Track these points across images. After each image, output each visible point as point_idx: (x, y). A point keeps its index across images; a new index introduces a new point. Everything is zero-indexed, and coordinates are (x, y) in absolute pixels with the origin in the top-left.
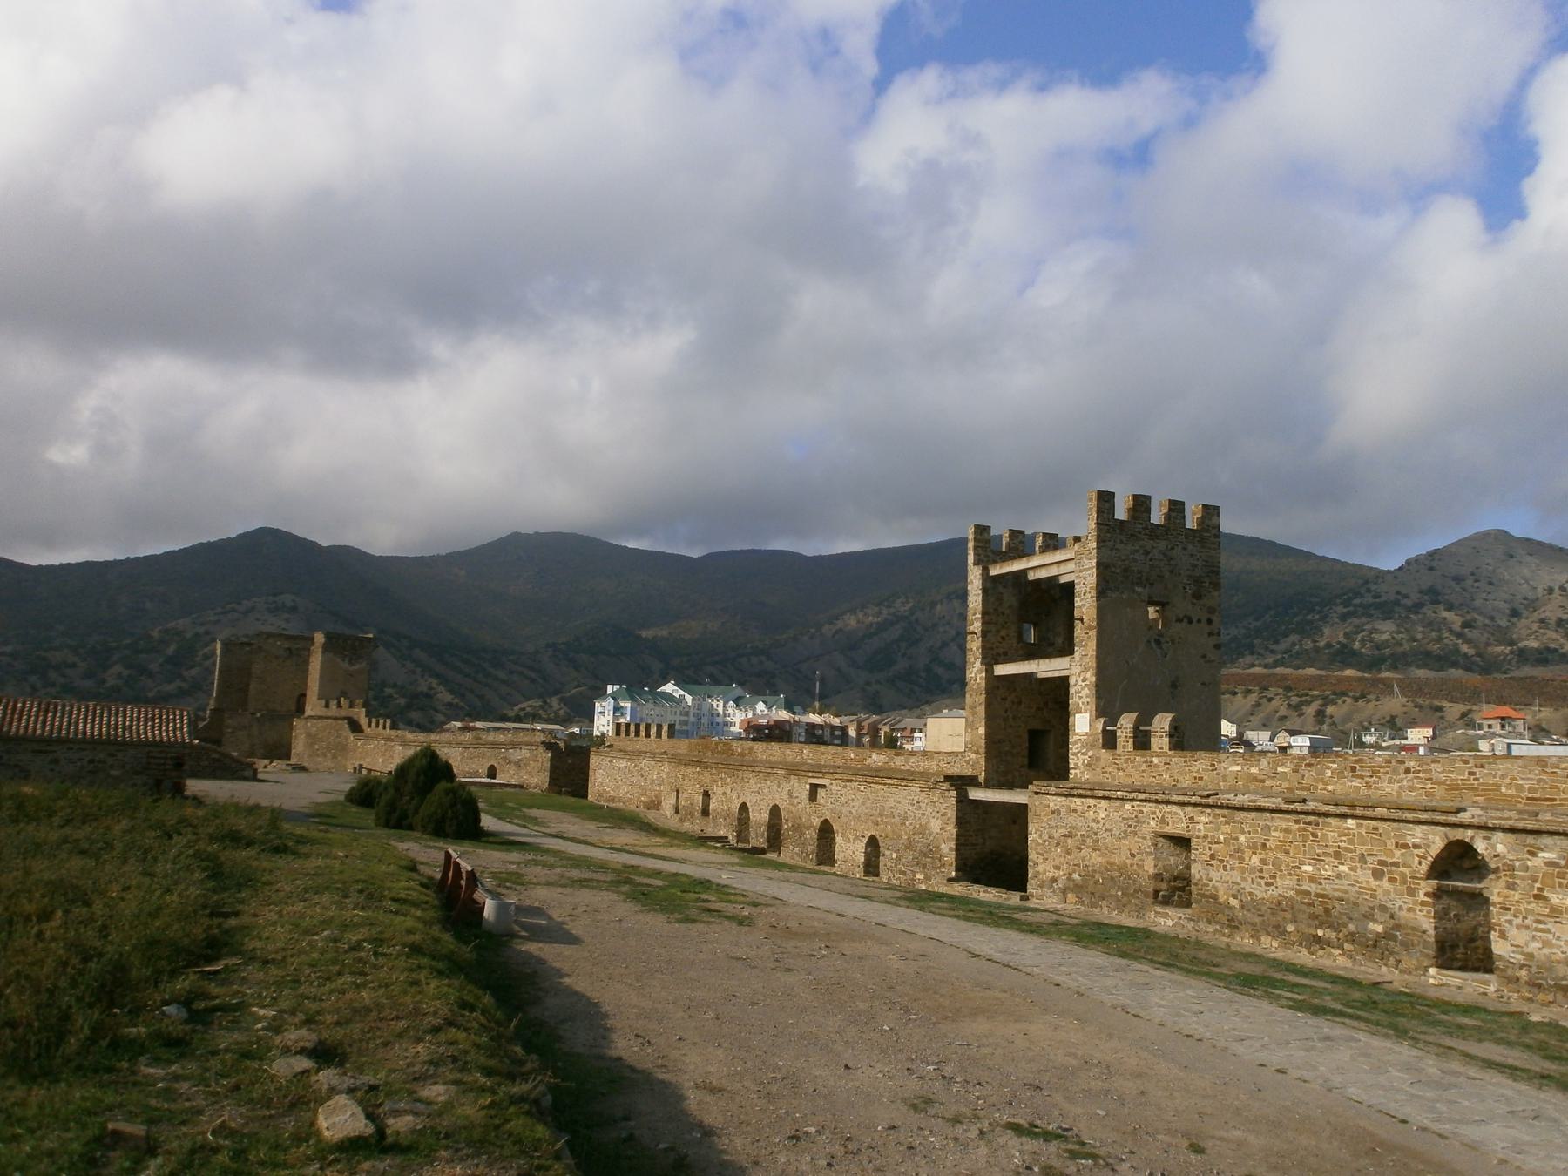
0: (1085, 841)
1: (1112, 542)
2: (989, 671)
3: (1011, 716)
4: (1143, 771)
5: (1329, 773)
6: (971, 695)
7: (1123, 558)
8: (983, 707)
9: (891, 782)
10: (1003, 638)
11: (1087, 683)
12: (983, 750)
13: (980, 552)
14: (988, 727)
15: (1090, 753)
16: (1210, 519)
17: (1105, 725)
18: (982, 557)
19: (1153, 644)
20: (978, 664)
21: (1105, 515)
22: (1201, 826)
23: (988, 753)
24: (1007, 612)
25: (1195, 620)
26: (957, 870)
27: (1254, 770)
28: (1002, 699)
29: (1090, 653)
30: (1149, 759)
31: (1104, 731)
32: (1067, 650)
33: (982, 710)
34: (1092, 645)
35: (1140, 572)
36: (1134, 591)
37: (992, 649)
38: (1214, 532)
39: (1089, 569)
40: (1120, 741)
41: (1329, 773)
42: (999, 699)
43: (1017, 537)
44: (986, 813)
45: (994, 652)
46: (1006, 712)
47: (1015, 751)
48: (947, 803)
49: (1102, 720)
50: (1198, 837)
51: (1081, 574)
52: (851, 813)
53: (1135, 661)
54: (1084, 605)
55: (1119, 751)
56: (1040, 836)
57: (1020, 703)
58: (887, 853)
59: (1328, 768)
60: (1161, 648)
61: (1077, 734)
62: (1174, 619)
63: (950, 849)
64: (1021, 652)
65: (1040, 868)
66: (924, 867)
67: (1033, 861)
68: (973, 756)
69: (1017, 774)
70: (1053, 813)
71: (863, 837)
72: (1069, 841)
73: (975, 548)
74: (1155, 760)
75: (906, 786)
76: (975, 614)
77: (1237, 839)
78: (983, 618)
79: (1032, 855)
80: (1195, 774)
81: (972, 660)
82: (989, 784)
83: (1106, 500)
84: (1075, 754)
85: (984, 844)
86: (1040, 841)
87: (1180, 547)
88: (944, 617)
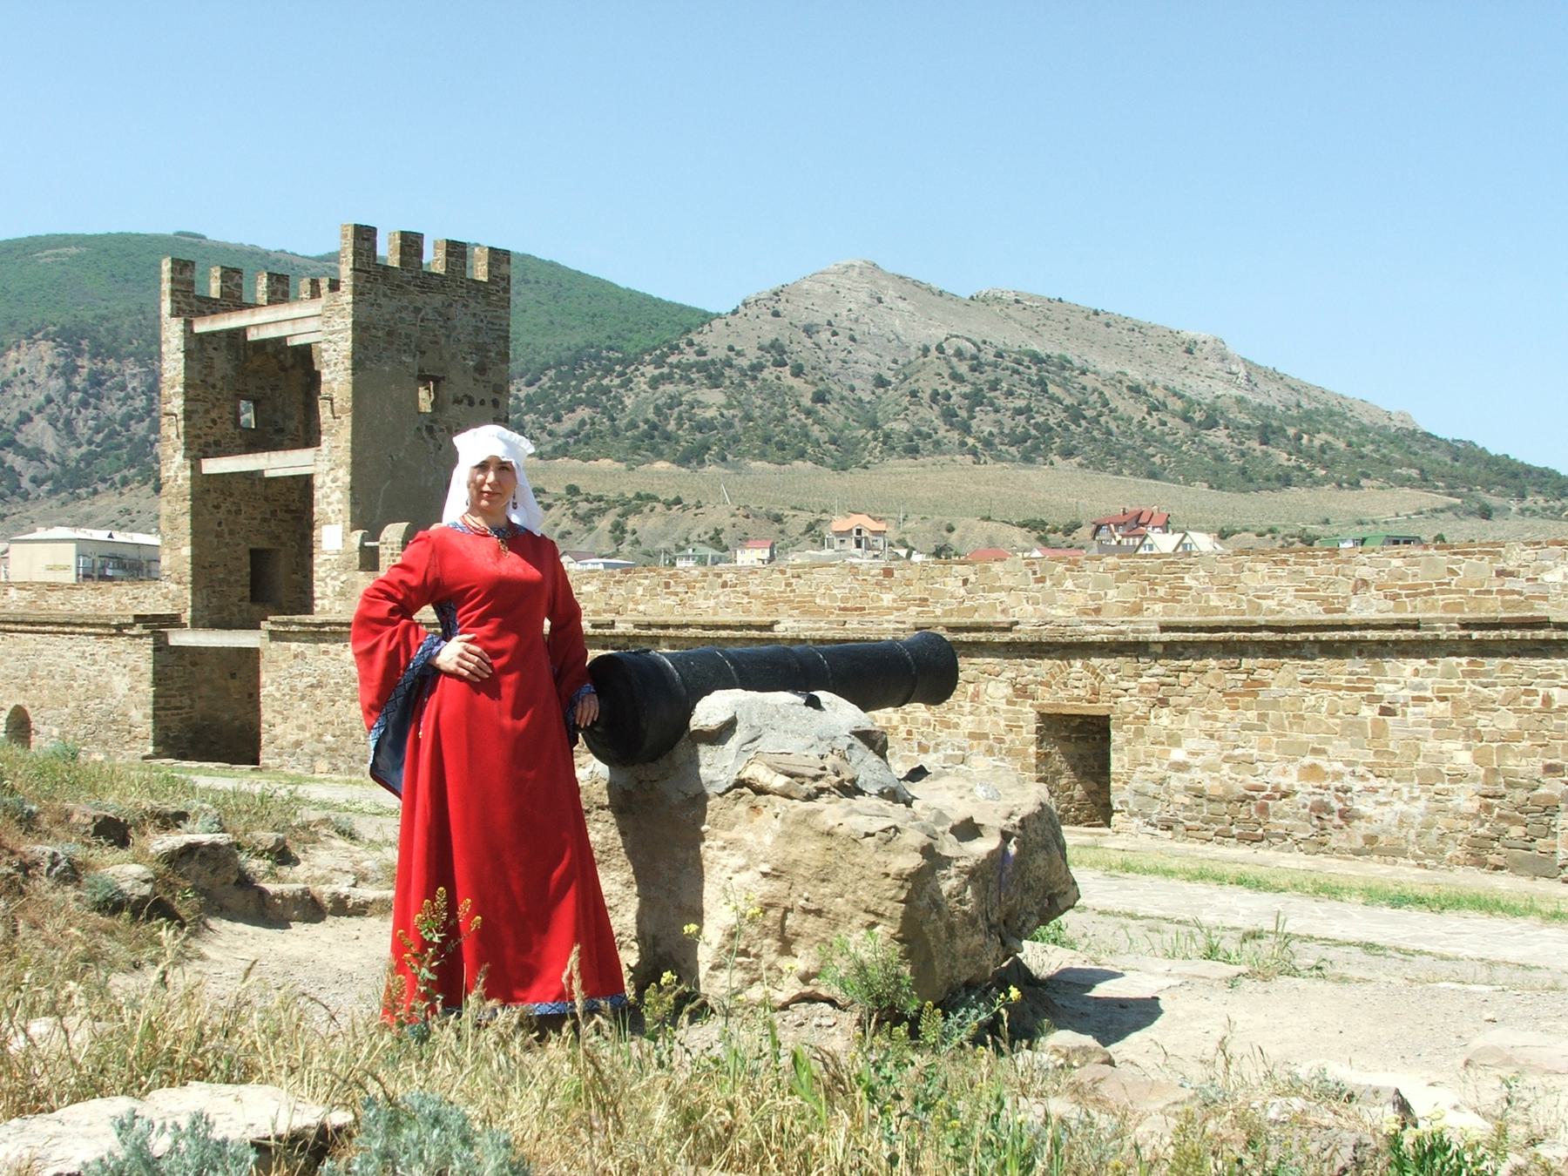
0: (340, 691)
1: (372, 295)
2: (196, 468)
3: (226, 531)
5: (640, 591)
6: (169, 502)
7: (387, 317)
8: (188, 518)
9: (49, 628)
10: (214, 422)
11: (339, 483)
13: (180, 298)
14: (194, 544)
15: (343, 578)
16: (498, 268)
17: (364, 538)
18: (183, 305)
19: (425, 434)
20: (179, 458)
21: (364, 259)
23: (194, 582)
24: (220, 384)
25: (477, 401)
26: (156, 744)
28: (214, 507)
31: (362, 548)
32: (309, 436)
33: (185, 522)
34: (346, 434)
35: (408, 336)
36: (401, 363)
37: (198, 437)
38: (503, 284)
39: (339, 331)
41: (640, 591)
42: (210, 506)
43: (232, 279)
44: (194, 664)
45: (202, 441)
46: (220, 524)
47: (232, 579)
48: (140, 655)
49: (359, 533)
51: (330, 337)
53: (401, 454)
54: (335, 379)
56: (278, 689)
57: (238, 512)
58: (44, 729)
59: (639, 585)
60: (433, 438)
62: (451, 398)
63: (145, 716)
64: (239, 441)
65: (278, 730)
66: (105, 743)
67: (267, 722)
68: (174, 587)
69: (235, 610)
70: (296, 656)
72: (318, 692)
73: (173, 292)
75: (72, 633)
76: (173, 387)
78: (186, 393)
79: (266, 715)
81: (170, 452)
82: (196, 624)
83: (364, 236)
84: (323, 580)
85: (191, 707)
86: (278, 695)
87: (460, 304)
88: (23, 371)
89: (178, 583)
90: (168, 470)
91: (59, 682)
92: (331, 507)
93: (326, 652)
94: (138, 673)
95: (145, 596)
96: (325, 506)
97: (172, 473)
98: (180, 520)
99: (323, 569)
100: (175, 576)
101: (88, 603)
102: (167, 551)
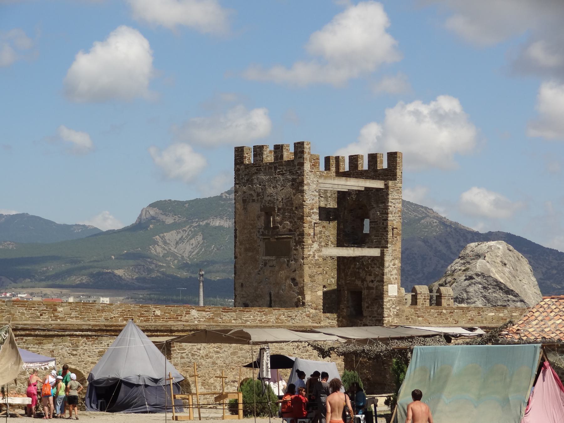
4: (436, 317)
6: (310, 268)
11: (395, 266)
15: (398, 308)
27: (501, 315)
29: (398, 250)
30: (440, 311)
34: (399, 245)
52: (214, 363)
55: (418, 307)
71: (234, 382)
74: (444, 311)
76: (312, 209)
80: (469, 318)
84: (389, 309)
89: (316, 309)
90: (309, 251)
92: (392, 276)
95: (296, 316)
97: (311, 253)
99: (389, 304)
100: (314, 305)
101: (256, 319)
102: (309, 292)
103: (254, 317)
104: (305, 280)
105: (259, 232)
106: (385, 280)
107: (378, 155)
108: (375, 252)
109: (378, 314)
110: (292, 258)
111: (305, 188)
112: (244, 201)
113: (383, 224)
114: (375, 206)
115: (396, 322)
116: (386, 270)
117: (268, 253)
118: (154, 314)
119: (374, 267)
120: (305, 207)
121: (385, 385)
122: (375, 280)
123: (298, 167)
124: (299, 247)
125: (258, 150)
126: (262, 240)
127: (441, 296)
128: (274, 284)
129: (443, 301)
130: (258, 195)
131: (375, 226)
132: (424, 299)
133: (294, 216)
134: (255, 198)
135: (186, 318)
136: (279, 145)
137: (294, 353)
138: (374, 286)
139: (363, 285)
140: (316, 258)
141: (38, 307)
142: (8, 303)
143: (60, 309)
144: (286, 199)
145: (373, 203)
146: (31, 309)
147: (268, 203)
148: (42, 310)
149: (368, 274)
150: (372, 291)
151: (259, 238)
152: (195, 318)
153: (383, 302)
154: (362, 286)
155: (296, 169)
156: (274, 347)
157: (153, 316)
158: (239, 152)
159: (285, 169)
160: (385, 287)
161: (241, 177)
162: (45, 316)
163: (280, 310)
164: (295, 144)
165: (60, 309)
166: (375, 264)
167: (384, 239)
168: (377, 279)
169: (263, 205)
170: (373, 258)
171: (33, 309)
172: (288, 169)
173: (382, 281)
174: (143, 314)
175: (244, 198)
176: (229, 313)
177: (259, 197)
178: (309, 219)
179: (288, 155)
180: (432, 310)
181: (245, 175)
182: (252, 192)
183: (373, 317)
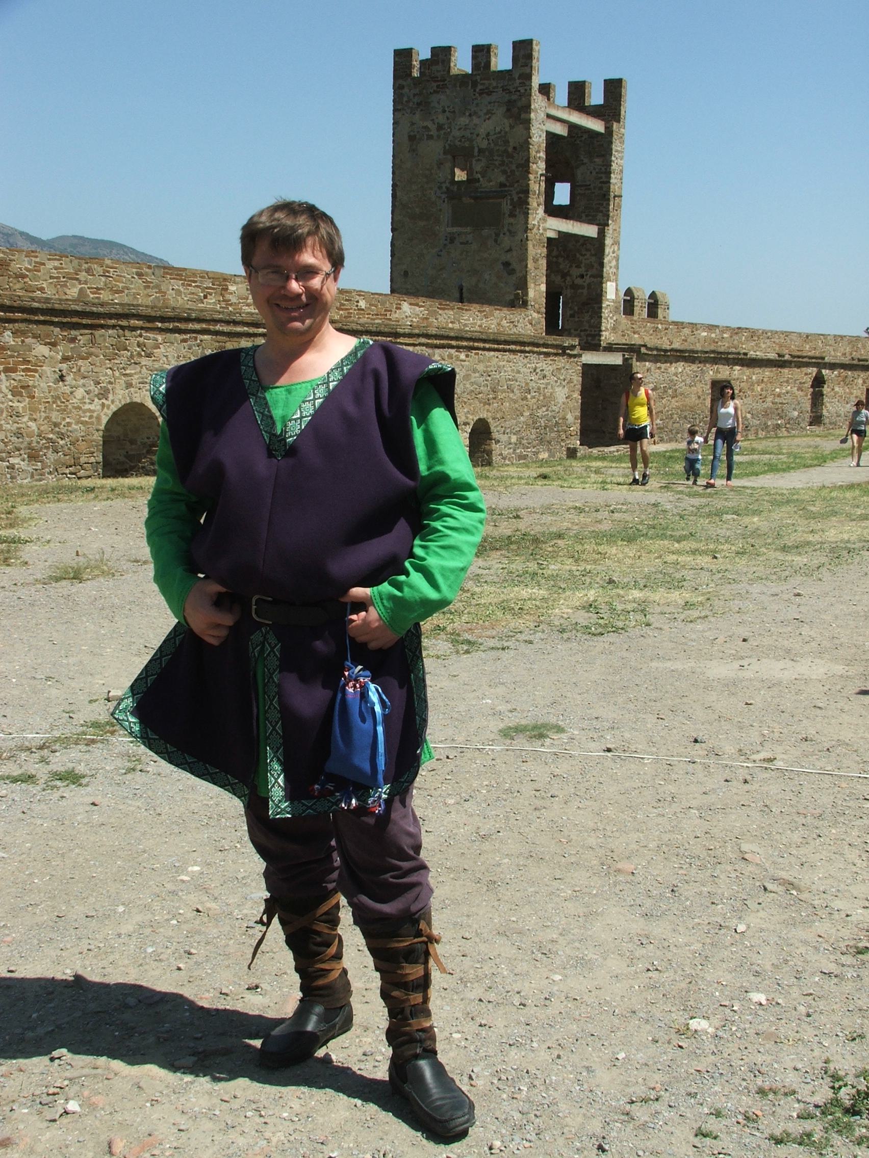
4: (651, 335)
6: (534, 246)
9: (513, 347)
12: (544, 310)
15: (615, 318)
22: (736, 372)
27: (713, 335)
30: (656, 326)
40: (637, 310)
50: (734, 380)
55: (635, 318)
61: (607, 300)
63: (575, 419)
74: (660, 326)
76: (538, 152)
77: (751, 378)
80: (683, 338)
89: (538, 313)
90: (534, 219)
91: (517, 394)
93: (660, 368)
94: (572, 385)
96: (608, 268)
97: (536, 222)
98: (540, 262)
102: (532, 285)
103: (473, 320)
104: (529, 266)
105: (440, 188)
106: (605, 275)
107: (587, 84)
108: (590, 231)
109: (590, 326)
110: (505, 229)
111: (532, 115)
112: (412, 138)
113: (601, 188)
114: (586, 161)
115: (613, 338)
116: (606, 261)
117: (455, 222)
118: (357, 306)
119: (585, 255)
120: (531, 147)
121: (604, 432)
122: (587, 275)
123: (521, 81)
124: (518, 210)
125: (442, 54)
126: (446, 202)
127: (658, 305)
128: (468, 271)
129: (660, 311)
130: (440, 127)
131: (587, 192)
132: (641, 307)
133: (511, 162)
134: (434, 132)
135: (397, 316)
136: (483, 46)
137: (531, 380)
138: (585, 284)
139: (565, 281)
140: (541, 231)
141: (201, 282)
142: (157, 272)
143: (232, 288)
144: (495, 134)
145: (582, 158)
146: (190, 285)
147: (460, 141)
148: (207, 288)
149: (574, 265)
150: (580, 291)
151: (440, 197)
152: (407, 317)
153: (601, 308)
154: (563, 284)
155: (515, 85)
156: (509, 369)
157: (355, 310)
158: (403, 57)
159: (495, 84)
160: (604, 285)
161: (405, 99)
162: (211, 299)
163: (501, 310)
164: (514, 43)
165: (232, 288)
166: (587, 250)
167: (602, 212)
168: (589, 273)
169: (450, 145)
170: (586, 239)
171: (193, 284)
172: (500, 85)
173: (601, 276)
174: (344, 305)
175: (412, 134)
176: (446, 311)
177: (442, 132)
178: (534, 166)
179: (502, 61)
180: (648, 324)
181: (415, 95)
182: (428, 124)
183: (581, 331)
